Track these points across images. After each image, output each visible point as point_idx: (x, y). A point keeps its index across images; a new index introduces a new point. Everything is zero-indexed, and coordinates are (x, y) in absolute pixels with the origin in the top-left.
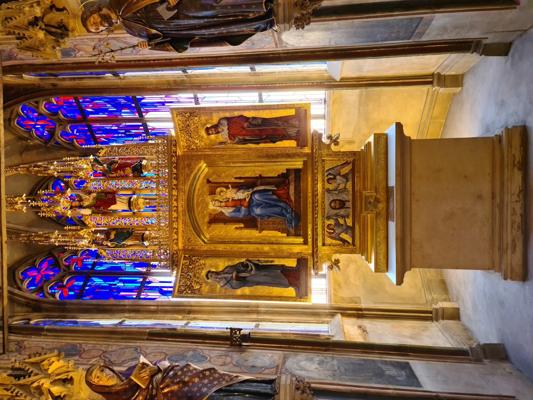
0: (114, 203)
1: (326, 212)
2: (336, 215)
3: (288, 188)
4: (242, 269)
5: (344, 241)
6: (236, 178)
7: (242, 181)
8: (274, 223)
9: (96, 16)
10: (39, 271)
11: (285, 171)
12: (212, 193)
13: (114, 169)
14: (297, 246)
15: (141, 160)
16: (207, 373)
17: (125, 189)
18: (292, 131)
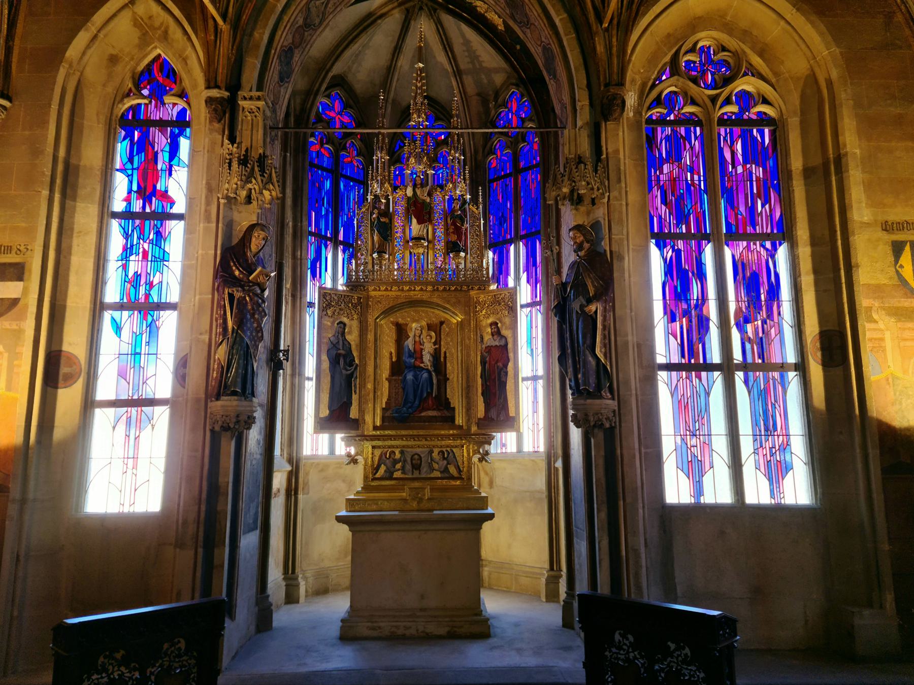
0: (419, 222)
1: (409, 450)
2: (405, 461)
3: (434, 410)
4: (348, 361)
5: (377, 469)
6: (445, 353)
7: (442, 359)
8: (397, 393)
9: (582, 238)
10: (340, 113)
11: (452, 406)
12: (430, 327)
13: (455, 220)
14: (372, 418)
15: (465, 251)
16: (260, 334)
17: (434, 231)
18: (493, 414)
